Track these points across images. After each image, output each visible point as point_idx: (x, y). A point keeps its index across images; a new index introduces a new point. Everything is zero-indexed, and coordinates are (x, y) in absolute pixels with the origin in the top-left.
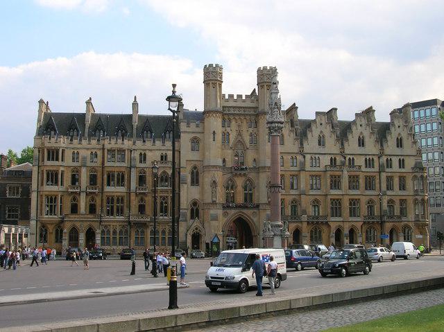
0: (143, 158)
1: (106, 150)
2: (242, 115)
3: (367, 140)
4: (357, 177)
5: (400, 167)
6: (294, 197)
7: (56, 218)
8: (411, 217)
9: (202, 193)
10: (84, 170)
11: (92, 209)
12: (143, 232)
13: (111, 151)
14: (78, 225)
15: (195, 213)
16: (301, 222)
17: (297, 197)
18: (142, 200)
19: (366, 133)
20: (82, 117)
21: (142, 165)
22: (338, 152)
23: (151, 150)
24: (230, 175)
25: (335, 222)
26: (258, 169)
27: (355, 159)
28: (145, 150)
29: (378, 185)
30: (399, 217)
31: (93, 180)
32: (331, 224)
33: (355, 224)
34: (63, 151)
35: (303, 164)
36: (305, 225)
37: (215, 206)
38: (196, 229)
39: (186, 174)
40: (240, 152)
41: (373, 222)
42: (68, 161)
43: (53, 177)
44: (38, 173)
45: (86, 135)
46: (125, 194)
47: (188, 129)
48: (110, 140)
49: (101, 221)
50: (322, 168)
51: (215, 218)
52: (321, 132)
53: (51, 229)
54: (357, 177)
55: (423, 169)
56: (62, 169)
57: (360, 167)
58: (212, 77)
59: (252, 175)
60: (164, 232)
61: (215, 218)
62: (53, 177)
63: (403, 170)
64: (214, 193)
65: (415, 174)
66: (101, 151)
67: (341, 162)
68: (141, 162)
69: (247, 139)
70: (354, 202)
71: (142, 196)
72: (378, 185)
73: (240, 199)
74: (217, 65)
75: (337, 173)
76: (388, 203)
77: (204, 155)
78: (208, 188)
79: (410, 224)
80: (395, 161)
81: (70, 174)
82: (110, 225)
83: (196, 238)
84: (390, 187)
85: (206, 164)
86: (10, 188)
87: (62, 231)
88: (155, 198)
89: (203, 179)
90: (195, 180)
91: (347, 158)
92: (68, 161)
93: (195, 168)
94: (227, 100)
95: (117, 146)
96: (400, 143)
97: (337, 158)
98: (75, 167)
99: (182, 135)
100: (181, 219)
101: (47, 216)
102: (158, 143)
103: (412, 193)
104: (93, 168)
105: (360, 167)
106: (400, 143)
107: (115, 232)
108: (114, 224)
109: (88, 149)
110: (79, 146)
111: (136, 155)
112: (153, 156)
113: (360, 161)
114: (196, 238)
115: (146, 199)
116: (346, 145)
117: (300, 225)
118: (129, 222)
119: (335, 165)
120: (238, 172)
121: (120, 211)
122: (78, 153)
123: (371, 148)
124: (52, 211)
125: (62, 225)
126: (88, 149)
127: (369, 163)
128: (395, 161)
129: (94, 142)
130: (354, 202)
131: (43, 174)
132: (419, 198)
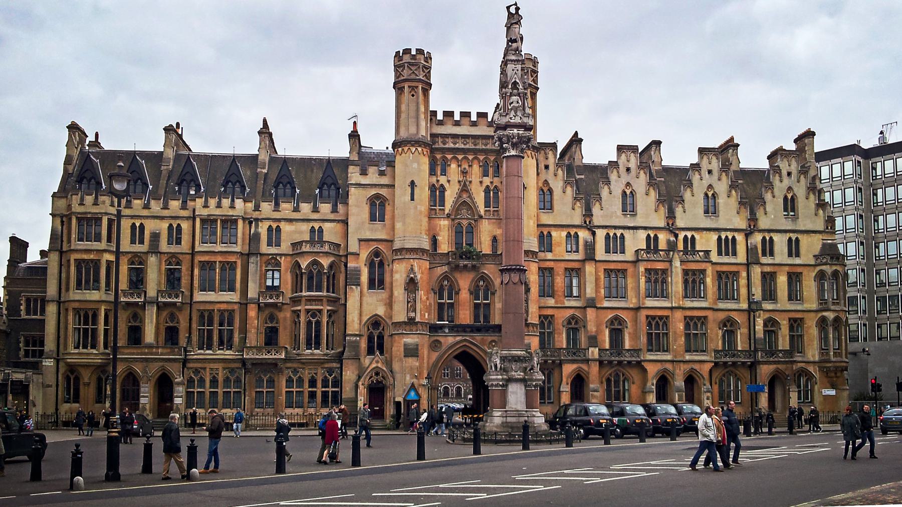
3: (722, 200)
5: (790, 255)
7: (95, 355)
8: (812, 353)
9: (390, 304)
10: (152, 260)
11: (171, 335)
12: (271, 382)
13: (208, 221)
14: (138, 369)
16: (587, 361)
17: (578, 313)
18: (272, 318)
19: (722, 187)
20: (155, 158)
22: (662, 223)
23: (290, 221)
24: (445, 268)
25: (654, 362)
27: (697, 236)
28: (279, 220)
30: (789, 353)
31: (172, 279)
33: (696, 367)
35: (590, 248)
36: (594, 369)
37: (414, 328)
38: (377, 374)
40: (465, 223)
41: (734, 363)
43: (88, 274)
45: (162, 192)
46: (236, 307)
47: (364, 180)
49: (185, 362)
50: (629, 256)
51: (411, 352)
53: (86, 376)
54: (703, 272)
55: (838, 259)
57: (707, 253)
58: (412, 73)
60: (313, 383)
62: (88, 274)
63: (798, 261)
64: (412, 306)
65: (824, 267)
66: (191, 222)
67: (669, 242)
69: (479, 199)
70: (695, 323)
72: (743, 291)
73: (465, 316)
74: (420, 51)
75: (660, 266)
76: (765, 325)
77: (393, 228)
78: (399, 293)
79: (811, 369)
80: (780, 242)
82: (205, 369)
83: (377, 392)
84: (770, 294)
85: (397, 245)
86: (28, 301)
88: (297, 314)
89: (392, 276)
90: (377, 282)
93: (377, 253)
94: (441, 123)
95: (218, 212)
96: (790, 204)
99: (352, 190)
101: (76, 351)
102: (306, 208)
103: (814, 306)
104: (173, 255)
105: (707, 253)
106: (790, 204)
107: (214, 382)
108: (212, 366)
109: (162, 218)
110: (145, 213)
112: (292, 233)
113: (707, 242)
114: (377, 392)
115: (281, 315)
116: (679, 210)
117: (584, 367)
119: (656, 250)
120: (462, 263)
121: (226, 342)
123: (731, 216)
124: (87, 338)
127: (726, 246)
128: (780, 242)
129: (175, 204)
130: (695, 324)
131: (69, 267)
132: (830, 316)
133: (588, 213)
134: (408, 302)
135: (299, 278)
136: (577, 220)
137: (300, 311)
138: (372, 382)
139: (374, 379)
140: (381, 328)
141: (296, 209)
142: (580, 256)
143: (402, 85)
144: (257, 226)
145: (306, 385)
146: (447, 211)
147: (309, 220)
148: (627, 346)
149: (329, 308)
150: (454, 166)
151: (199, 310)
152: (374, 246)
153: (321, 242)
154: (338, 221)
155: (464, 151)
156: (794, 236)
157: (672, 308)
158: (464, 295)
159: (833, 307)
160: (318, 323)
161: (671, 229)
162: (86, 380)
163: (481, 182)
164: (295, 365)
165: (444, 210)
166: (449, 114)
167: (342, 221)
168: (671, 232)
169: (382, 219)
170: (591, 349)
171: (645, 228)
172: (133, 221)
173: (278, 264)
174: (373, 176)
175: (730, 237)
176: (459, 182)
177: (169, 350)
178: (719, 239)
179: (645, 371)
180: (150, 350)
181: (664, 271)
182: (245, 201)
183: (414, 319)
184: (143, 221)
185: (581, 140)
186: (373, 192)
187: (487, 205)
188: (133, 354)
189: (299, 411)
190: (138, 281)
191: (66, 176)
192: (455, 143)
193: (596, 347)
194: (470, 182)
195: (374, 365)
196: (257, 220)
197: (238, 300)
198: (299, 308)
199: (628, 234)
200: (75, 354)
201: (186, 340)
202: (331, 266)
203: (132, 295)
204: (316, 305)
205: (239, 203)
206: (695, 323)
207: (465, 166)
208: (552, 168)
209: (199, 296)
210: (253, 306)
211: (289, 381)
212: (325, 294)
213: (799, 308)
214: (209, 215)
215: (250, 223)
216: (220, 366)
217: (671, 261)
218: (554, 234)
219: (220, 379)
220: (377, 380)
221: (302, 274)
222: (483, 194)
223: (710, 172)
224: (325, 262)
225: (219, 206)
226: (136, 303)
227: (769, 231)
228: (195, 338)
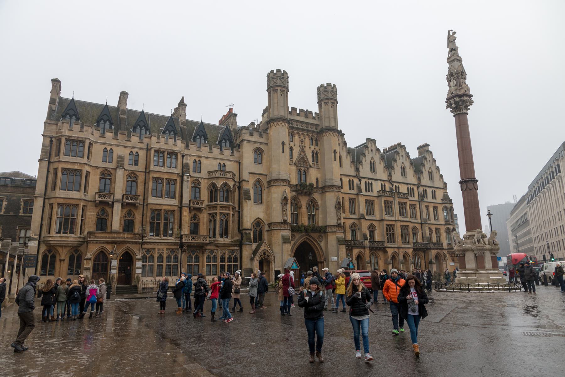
0: (198, 164)
1: (153, 151)
2: (305, 130)
4: (405, 203)
6: (352, 221)
7: (73, 238)
11: (128, 226)
12: (197, 259)
13: (159, 152)
14: (109, 248)
15: (259, 237)
16: (364, 248)
17: (356, 221)
21: (196, 175)
22: (387, 179)
24: (294, 193)
26: (324, 189)
27: (400, 186)
28: (201, 157)
29: (418, 214)
32: (387, 249)
33: (407, 250)
34: (90, 144)
37: (286, 226)
38: (264, 253)
39: (249, 186)
40: (303, 169)
42: (97, 159)
44: (48, 172)
46: (176, 208)
47: (251, 139)
48: (159, 138)
49: (143, 243)
50: (375, 193)
51: (286, 240)
52: (372, 158)
54: (405, 203)
56: (87, 168)
59: (316, 196)
61: (286, 240)
63: (435, 201)
66: (145, 152)
67: (390, 188)
68: (195, 171)
71: (196, 211)
72: (418, 214)
73: (304, 220)
74: (285, 72)
75: (390, 199)
80: (429, 191)
82: (154, 249)
87: (79, 258)
88: (213, 216)
91: (394, 186)
92: (97, 159)
93: (258, 181)
94: (290, 113)
95: (166, 147)
98: (106, 169)
101: (59, 235)
102: (216, 151)
104: (133, 172)
108: (160, 247)
109: (126, 147)
112: (210, 165)
116: (393, 173)
117: (362, 250)
118: (182, 245)
122: (112, 151)
123: (411, 178)
125: (82, 249)
126: (126, 147)
129: (135, 139)
131: (56, 173)
134: (283, 211)
136: (353, 173)
137: (216, 214)
141: (211, 151)
142: (355, 192)
143: (276, 88)
144: (186, 159)
145: (219, 260)
147: (217, 159)
150: (297, 137)
151: (151, 209)
152: (257, 177)
153: (225, 172)
154: (234, 161)
155: (303, 130)
156: (434, 189)
157: (396, 221)
158: (304, 209)
159: (451, 223)
160: (227, 221)
161: (390, 181)
162: (63, 257)
164: (213, 248)
166: (294, 109)
167: (237, 162)
170: (366, 241)
171: (380, 180)
172: (105, 146)
173: (199, 184)
174: (256, 138)
177: (132, 236)
179: (386, 252)
180: (119, 235)
181: (391, 202)
184: (112, 147)
186: (256, 146)
187: (313, 161)
188: (106, 237)
191: (51, 112)
192: (297, 125)
197: (177, 204)
200: (55, 237)
204: (226, 210)
205: (179, 142)
206: (404, 228)
207: (302, 137)
208: (341, 144)
209: (151, 200)
210: (186, 208)
211: (208, 258)
213: (438, 223)
216: (165, 247)
219: (165, 256)
221: (216, 191)
222: (311, 154)
226: (106, 203)
227: (425, 186)
228: (148, 228)
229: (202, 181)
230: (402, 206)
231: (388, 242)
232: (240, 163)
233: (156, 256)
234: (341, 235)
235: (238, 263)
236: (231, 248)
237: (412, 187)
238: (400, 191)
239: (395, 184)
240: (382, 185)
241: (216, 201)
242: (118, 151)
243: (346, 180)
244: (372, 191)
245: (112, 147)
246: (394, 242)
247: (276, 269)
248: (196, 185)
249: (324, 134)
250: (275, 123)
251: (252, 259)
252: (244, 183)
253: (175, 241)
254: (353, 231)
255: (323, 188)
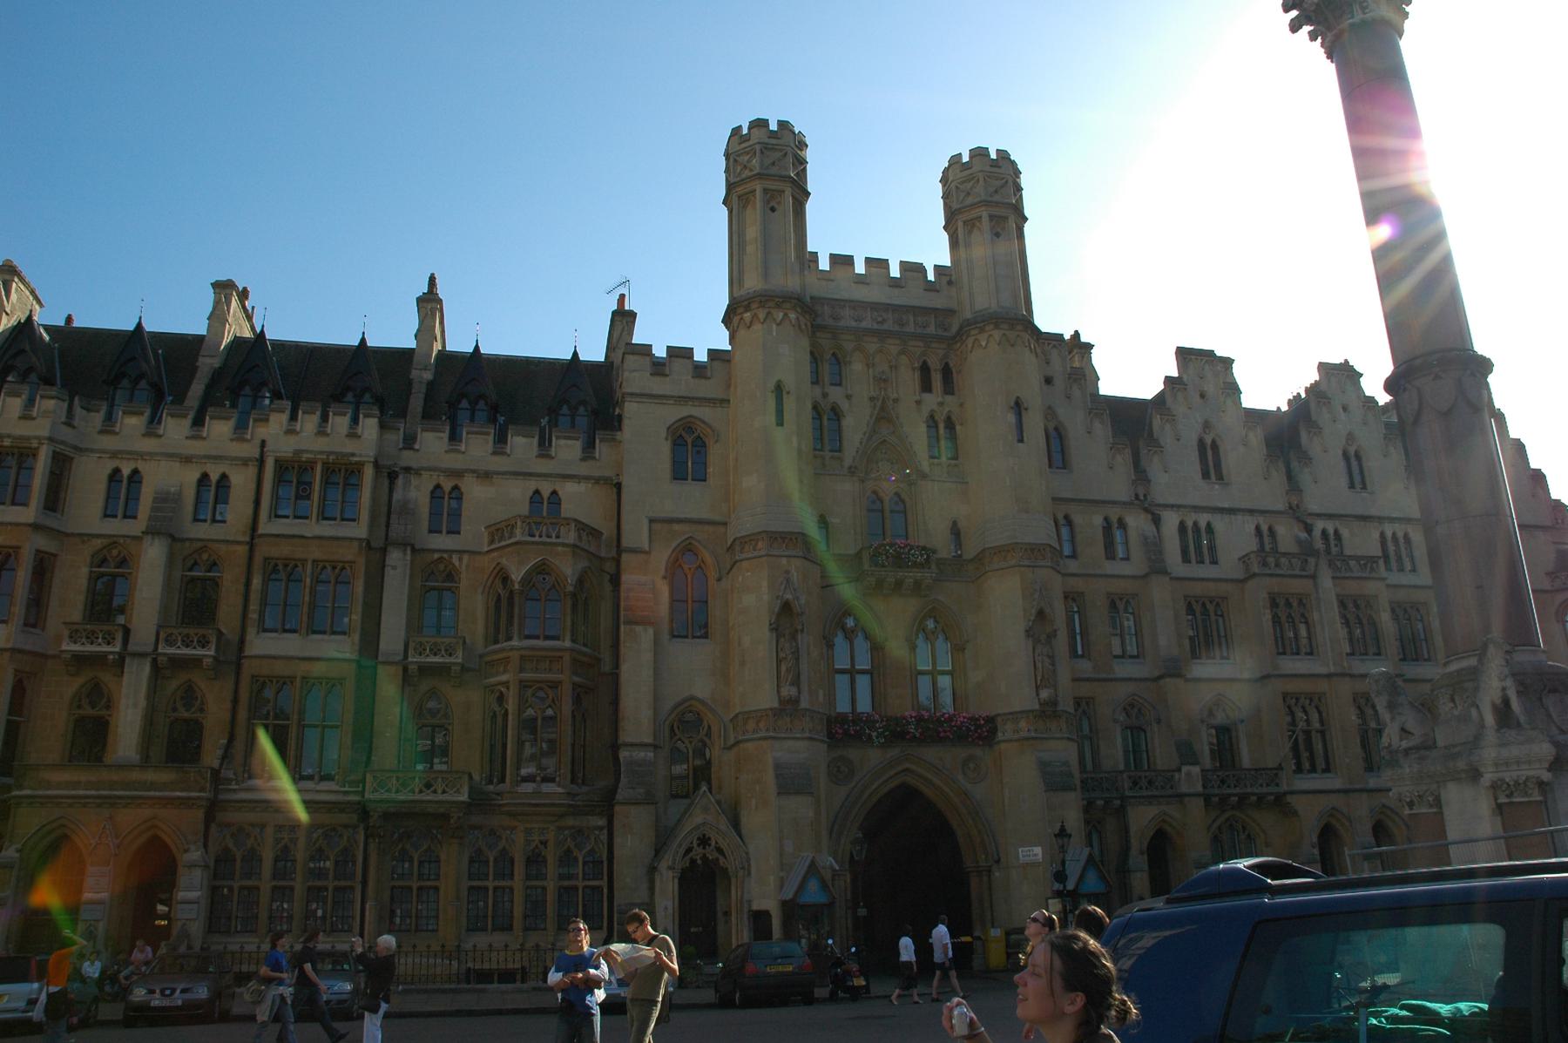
3: (1373, 463)
16: (1181, 797)
21: (441, 541)
22: (1280, 506)
27: (1345, 533)
31: (194, 602)
35: (1154, 548)
42: (87, 508)
48: (293, 417)
50: (1229, 565)
52: (1207, 425)
66: (252, 471)
67: (1299, 542)
74: (783, 125)
75: (1297, 586)
81: (85, 570)
93: (688, 548)
95: (321, 444)
97: (1281, 530)
98: (113, 541)
99: (630, 409)
100: (621, 794)
109: (187, 460)
111: (417, 493)
112: (491, 500)
116: (1305, 477)
126: (187, 460)
133: (1141, 475)
134: (779, 661)
135: (504, 603)
137: (506, 684)
138: (693, 861)
139: (698, 852)
140: (703, 733)
145: (519, 870)
146: (848, 462)
148: (1246, 760)
149: (576, 679)
150: (857, 366)
154: (596, 481)
157: (1329, 676)
163: (918, 403)
165: (841, 459)
166: (842, 261)
168: (1299, 520)
169: (701, 478)
170: (1185, 769)
171: (1251, 512)
173: (451, 576)
175: (1400, 535)
176: (872, 399)
178: (1382, 535)
182: (383, 426)
183: (797, 701)
185: (1089, 346)
189: (498, 939)
190: (104, 605)
192: (859, 320)
193: (1195, 763)
194: (896, 401)
195: (698, 820)
196: (407, 470)
198: (504, 678)
199: (1220, 524)
201: (220, 752)
202: (580, 581)
203: (91, 638)
205: (369, 427)
208: (1059, 382)
212: (568, 644)
214: (297, 452)
215: (392, 476)
217: (1314, 577)
218: (1077, 519)
220: (704, 857)
222: (923, 428)
223: (1345, 409)
224: (568, 569)
225: (321, 432)
226: (98, 660)
229: (461, 564)
230: (1354, 611)
231: (1299, 769)
232: (619, 486)
233: (268, 855)
234: (1063, 751)
235: (604, 883)
236: (570, 822)
237: (1400, 529)
238: (1347, 552)
239: (1319, 525)
240: (1258, 528)
241: (509, 638)
242: (162, 477)
243: (1090, 523)
244: (1214, 562)
245: (141, 465)
246: (1327, 770)
247: (755, 907)
248: (435, 580)
249: (970, 341)
250: (747, 315)
251: (652, 870)
252: (625, 557)
253: (340, 798)
254: (1136, 731)
255: (979, 558)
